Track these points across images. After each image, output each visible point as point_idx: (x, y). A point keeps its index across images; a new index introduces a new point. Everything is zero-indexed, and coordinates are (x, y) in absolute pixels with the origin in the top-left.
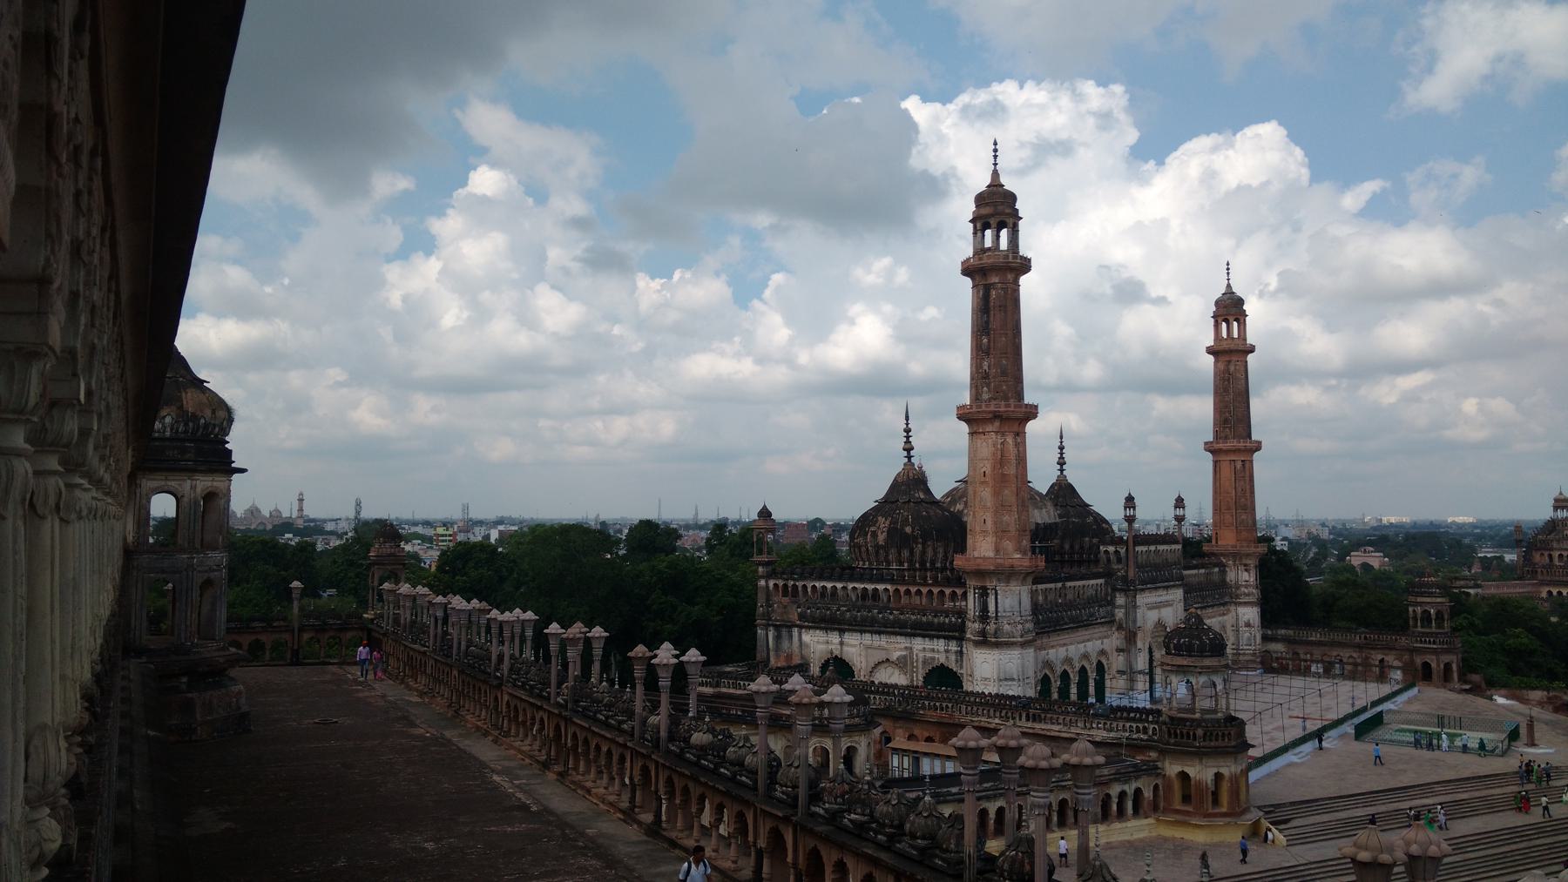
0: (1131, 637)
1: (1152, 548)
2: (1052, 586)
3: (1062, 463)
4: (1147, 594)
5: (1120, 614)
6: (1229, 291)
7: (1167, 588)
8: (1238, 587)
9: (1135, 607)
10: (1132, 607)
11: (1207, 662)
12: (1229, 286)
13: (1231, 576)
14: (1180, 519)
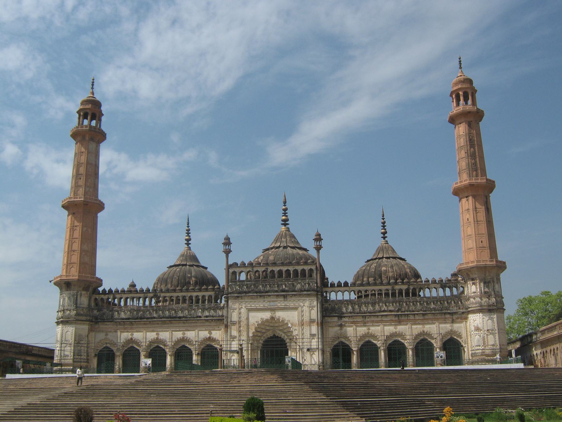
0: (226, 326)
7: (285, 297)
14: (318, 248)
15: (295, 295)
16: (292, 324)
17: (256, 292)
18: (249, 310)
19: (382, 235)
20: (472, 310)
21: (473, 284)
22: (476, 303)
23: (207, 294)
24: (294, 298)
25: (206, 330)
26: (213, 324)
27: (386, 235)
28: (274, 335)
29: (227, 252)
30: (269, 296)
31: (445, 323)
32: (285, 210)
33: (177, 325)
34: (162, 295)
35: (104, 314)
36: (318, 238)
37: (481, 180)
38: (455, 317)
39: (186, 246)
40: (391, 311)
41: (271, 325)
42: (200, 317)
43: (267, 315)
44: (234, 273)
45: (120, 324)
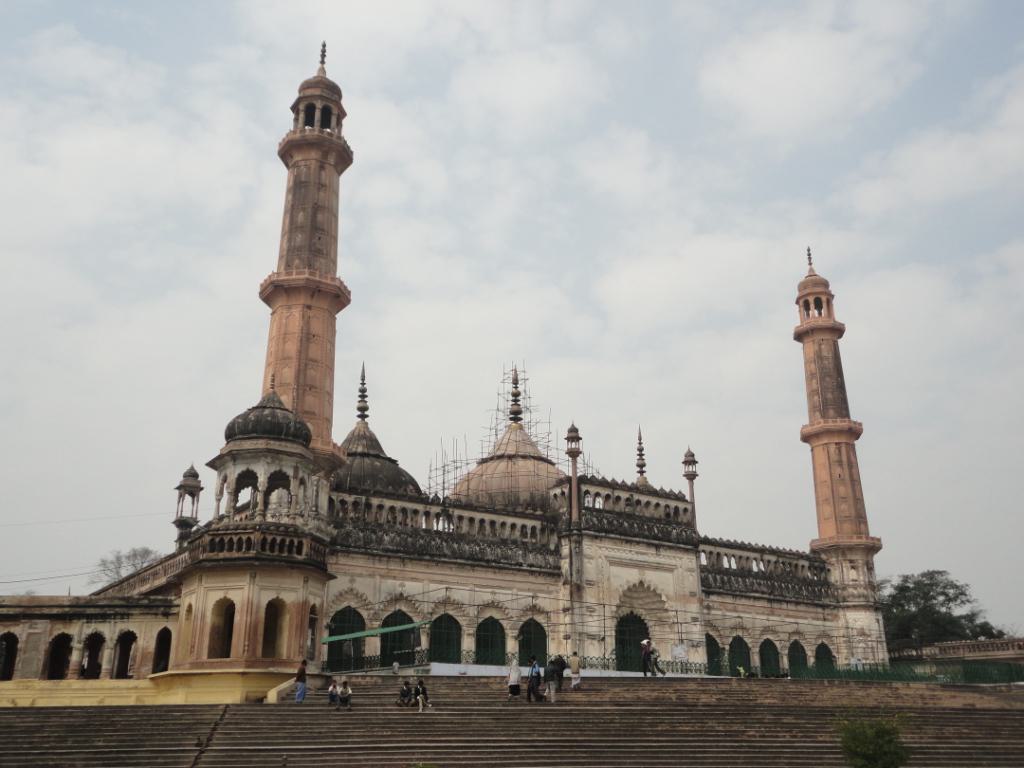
0: (577, 590)
1: (624, 495)
2: (420, 507)
3: (641, 466)
4: (607, 544)
5: (565, 565)
6: (812, 274)
7: (657, 547)
8: (844, 589)
9: (580, 553)
10: (577, 554)
11: (248, 445)
12: (811, 270)
13: (835, 576)
14: (691, 477)
15: (670, 548)
16: (667, 596)
17: (621, 534)
18: (614, 562)
19: (638, 469)
20: (854, 606)
21: (853, 567)
22: (859, 596)
23: (530, 523)
24: (669, 553)
25: (529, 590)
26: (541, 580)
27: (644, 469)
28: (632, 613)
29: (574, 454)
30: (638, 543)
31: (818, 619)
32: (516, 395)
33: (483, 575)
34: (457, 512)
35: (348, 534)
36: (690, 460)
37: (840, 424)
38: (827, 611)
39: (360, 419)
40: (763, 593)
41: (629, 594)
42: (521, 565)
43: (632, 576)
44: (587, 492)
45: (380, 561)
